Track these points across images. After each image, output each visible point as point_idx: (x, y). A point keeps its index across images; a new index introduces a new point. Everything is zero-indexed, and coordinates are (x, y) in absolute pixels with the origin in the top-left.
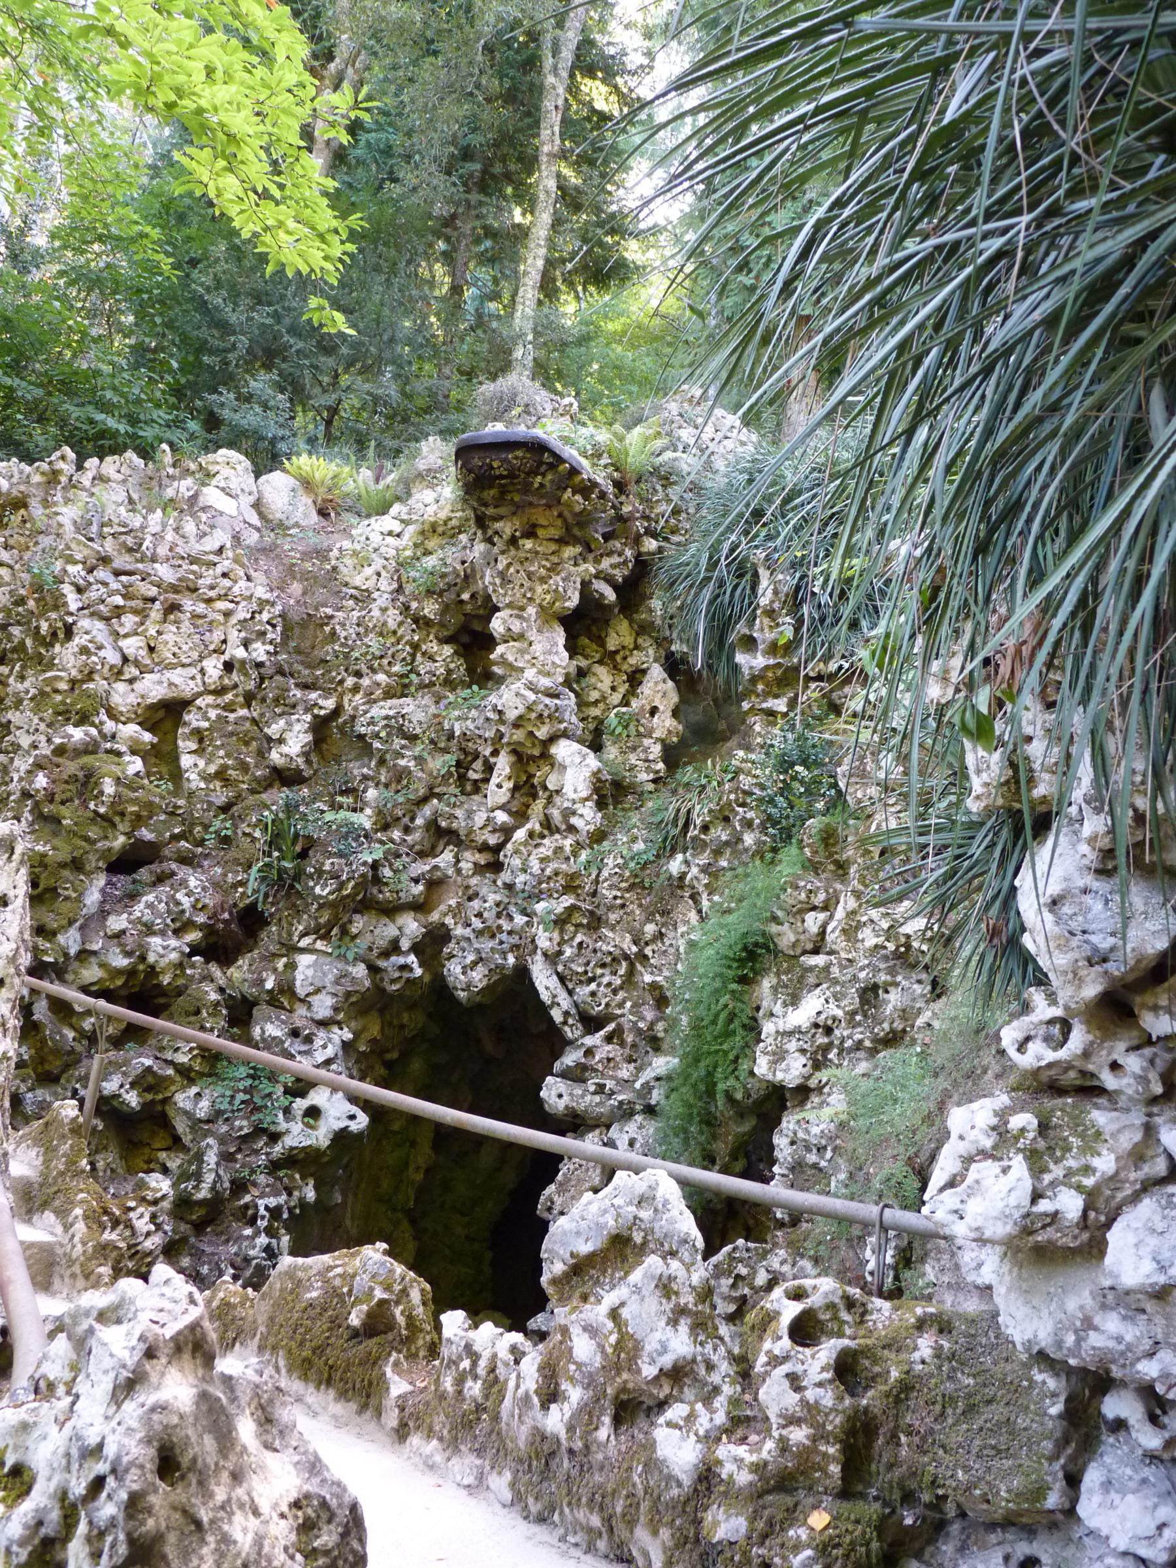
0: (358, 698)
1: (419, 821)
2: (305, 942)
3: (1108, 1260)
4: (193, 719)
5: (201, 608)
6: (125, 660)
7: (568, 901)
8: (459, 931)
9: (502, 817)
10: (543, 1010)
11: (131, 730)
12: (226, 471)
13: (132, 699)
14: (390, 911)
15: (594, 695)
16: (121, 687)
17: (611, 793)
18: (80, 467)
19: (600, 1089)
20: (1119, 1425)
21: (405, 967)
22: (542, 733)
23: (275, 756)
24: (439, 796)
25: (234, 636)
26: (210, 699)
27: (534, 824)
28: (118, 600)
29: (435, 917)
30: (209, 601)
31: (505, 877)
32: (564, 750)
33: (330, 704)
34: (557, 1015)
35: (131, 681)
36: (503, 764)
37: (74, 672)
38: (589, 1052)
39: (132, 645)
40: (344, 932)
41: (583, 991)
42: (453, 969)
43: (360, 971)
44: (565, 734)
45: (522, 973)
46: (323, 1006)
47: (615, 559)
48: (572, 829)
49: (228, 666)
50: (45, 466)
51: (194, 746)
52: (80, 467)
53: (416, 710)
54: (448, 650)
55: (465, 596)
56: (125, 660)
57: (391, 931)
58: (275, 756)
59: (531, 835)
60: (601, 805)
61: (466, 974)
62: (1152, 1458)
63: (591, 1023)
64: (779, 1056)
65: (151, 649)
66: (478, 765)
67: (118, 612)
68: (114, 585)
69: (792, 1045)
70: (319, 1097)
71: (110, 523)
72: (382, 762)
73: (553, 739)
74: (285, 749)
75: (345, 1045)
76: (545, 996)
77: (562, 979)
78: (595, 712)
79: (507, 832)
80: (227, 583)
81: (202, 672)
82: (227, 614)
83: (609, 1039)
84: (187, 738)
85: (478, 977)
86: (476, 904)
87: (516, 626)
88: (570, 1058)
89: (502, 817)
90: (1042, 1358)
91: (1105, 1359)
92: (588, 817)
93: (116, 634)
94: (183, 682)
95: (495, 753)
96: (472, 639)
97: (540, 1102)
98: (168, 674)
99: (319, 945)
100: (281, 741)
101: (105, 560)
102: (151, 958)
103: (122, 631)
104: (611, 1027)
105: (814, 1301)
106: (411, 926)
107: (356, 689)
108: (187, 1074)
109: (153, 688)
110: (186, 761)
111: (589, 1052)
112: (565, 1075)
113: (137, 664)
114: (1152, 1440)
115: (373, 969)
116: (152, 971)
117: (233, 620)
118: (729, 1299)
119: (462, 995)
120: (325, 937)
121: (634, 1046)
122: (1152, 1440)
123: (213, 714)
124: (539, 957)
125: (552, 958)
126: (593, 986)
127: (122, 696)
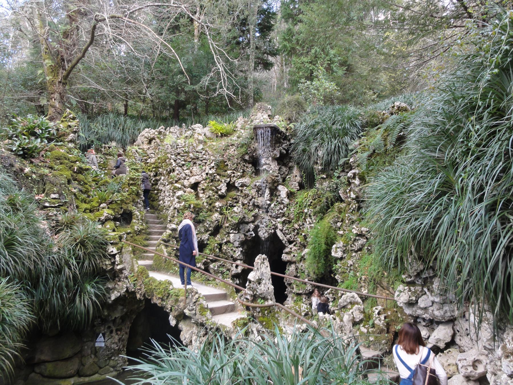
0: (235, 179)
1: (251, 204)
2: (231, 232)
3: (419, 304)
4: (200, 185)
5: (200, 162)
6: (186, 175)
7: (284, 218)
8: (261, 226)
9: (268, 202)
10: (280, 241)
11: (189, 189)
12: (198, 129)
13: (188, 183)
14: (248, 223)
15: (282, 173)
16: (186, 181)
17: (290, 195)
18: (165, 130)
19: (294, 256)
20: (420, 322)
21: (252, 234)
22: (276, 185)
23: (219, 193)
24: (254, 198)
25: (208, 168)
26: (204, 181)
27: (275, 203)
28: (183, 162)
29: (256, 223)
30: (201, 161)
31: (269, 214)
32: (280, 187)
33: (229, 180)
34: (284, 242)
35: (188, 180)
36: (267, 191)
37: (176, 179)
38: (291, 248)
39: (187, 172)
40: (239, 228)
41: (288, 236)
42: (261, 234)
43: (243, 236)
44: (280, 184)
45: (275, 233)
46: (237, 244)
47: (285, 145)
48: (283, 203)
49: (207, 174)
50: (158, 130)
51: (202, 192)
52: (165, 130)
53: (246, 180)
54: (251, 165)
55: (254, 154)
56: (186, 175)
57: (249, 227)
58: (219, 193)
59: (275, 205)
60: (288, 198)
61: (263, 234)
62: (424, 326)
63: (290, 242)
64: (336, 252)
65: (191, 172)
66: (261, 191)
67: (183, 165)
68: (182, 159)
69: (338, 250)
70: (238, 262)
71: (178, 145)
72: (242, 192)
73: (278, 185)
74: (222, 191)
75: (241, 251)
76: (281, 238)
77: (284, 234)
78: (283, 176)
79: (270, 205)
80: (205, 156)
81: (202, 176)
82: (206, 163)
83: (295, 245)
84: (200, 190)
85: (266, 235)
86: (264, 220)
87: (268, 162)
88: (287, 250)
89: (268, 202)
90: (410, 315)
91: (419, 315)
92: (286, 201)
93: (184, 170)
94: (198, 178)
95: (265, 189)
96: (255, 162)
97: (281, 259)
98: (195, 177)
99: (234, 232)
100: (221, 190)
101: (179, 154)
102: (203, 239)
103: (185, 169)
104: (295, 243)
105: (379, 309)
106: (252, 226)
107: (234, 176)
108: (213, 261)
109: (193, 180)
110: (201, 195)
111: (291, 248)
112: (287, 253)
113: (189, 176)
114: (424, 324)
115: (245, 235)
116: (203, 241)
117: (207, 164)
118: (332, 298)
119: (263, 239)
120: (236, 230)
121: (300, 247)
122: (424, 324)
123: (206, 185)
124: (278, 230)
125: (281, 230)
126: (290, 235)
127: (186, 183)
